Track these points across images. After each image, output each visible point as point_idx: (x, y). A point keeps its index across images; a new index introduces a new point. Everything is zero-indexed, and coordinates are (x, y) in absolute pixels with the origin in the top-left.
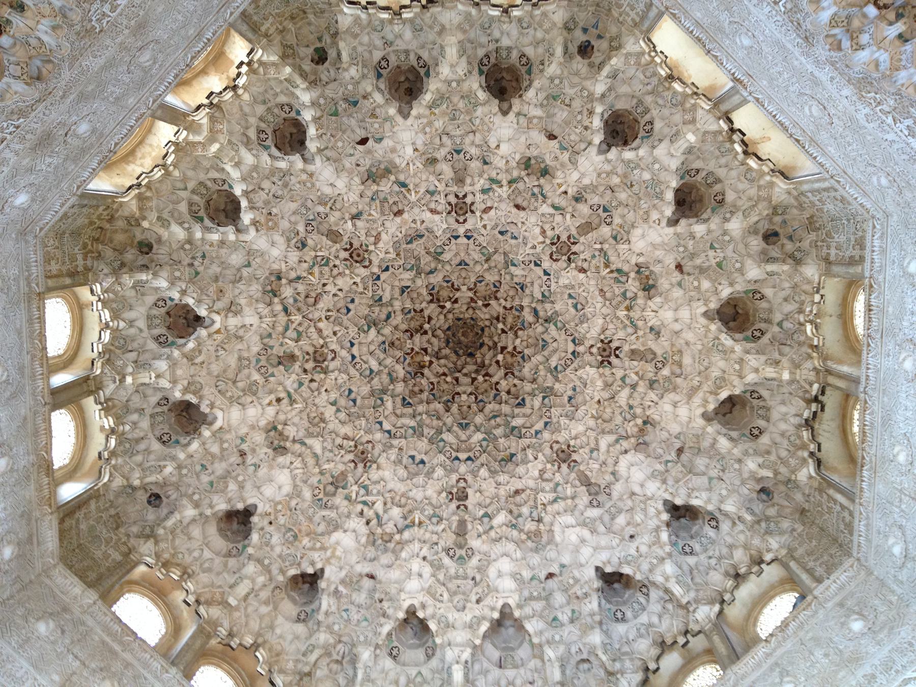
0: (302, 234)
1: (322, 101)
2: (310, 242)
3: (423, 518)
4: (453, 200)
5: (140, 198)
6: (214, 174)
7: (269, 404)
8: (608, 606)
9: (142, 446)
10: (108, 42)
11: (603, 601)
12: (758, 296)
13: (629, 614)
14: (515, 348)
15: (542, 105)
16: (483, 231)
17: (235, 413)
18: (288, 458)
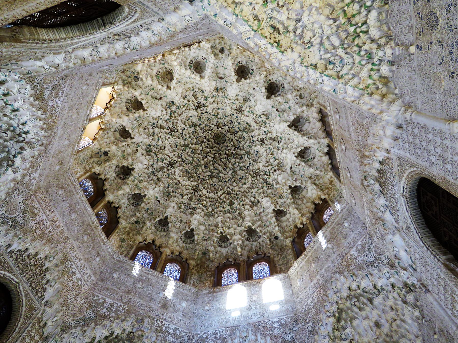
0: (192, 210)
1: (149, 219)
2: (194, 206)
3: (270, 154)
4: (169, 168)
5: (190, 260)
6: (179, 240)
7: (244, 208)
8: (280, 91)
9: (261, 243)
10: (133, 301)
11: (279, 93)
12: (158, 73)
13: (281, 83)
14: (215, 126)
15: (127, 159)
16: (177, 154)
17: (247, 218)
18: (260, 200)
